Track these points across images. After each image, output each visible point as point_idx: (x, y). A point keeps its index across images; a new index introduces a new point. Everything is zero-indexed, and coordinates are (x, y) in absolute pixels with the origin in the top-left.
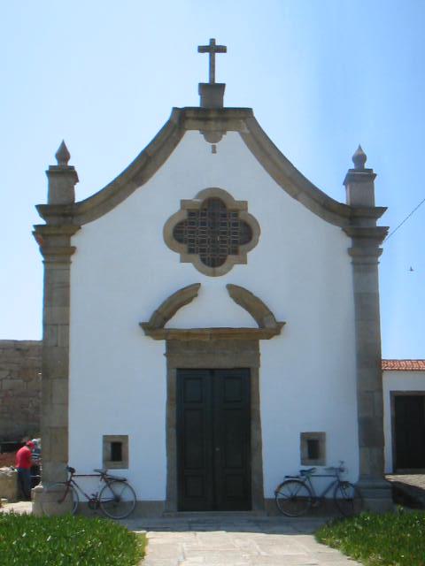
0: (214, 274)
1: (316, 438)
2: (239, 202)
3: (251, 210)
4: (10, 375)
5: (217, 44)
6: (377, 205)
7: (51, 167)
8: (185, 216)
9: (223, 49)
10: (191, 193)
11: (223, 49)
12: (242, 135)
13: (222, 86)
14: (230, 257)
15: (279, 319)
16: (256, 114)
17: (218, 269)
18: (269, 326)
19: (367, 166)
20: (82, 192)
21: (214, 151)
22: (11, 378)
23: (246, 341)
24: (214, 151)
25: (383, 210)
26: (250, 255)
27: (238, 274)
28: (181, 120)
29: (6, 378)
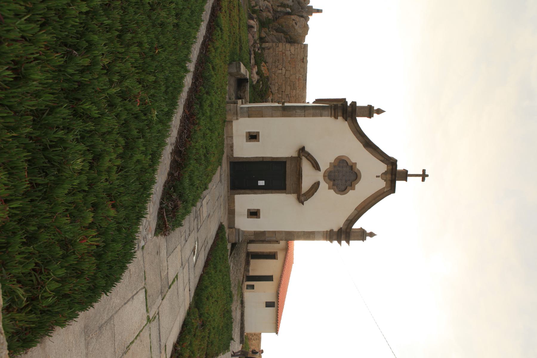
0: (324, 176)
1: (258, 214)
2: (355, 186)
3: (351, 191)
4: (292, 54)
5: (426, 178)
6: (351, 242)
7: (374, 107)
8: (350, 164)
9: (423, 180)
11: (423, 180)
12: (384, 188)
13: (406, 180)
14: (332, 183)
15: (305, 203)
17: (327, 178)
18: (302, 198)
19: (368, 238)
20: (362, 122)
21: (377, 177)
22: (291, 55)
23: (297, 189)
24: (377, 177)
25: (348, 242)
26: (332, 191)
27: (324, 185)
28: (392, 163)
29: (291, 53)
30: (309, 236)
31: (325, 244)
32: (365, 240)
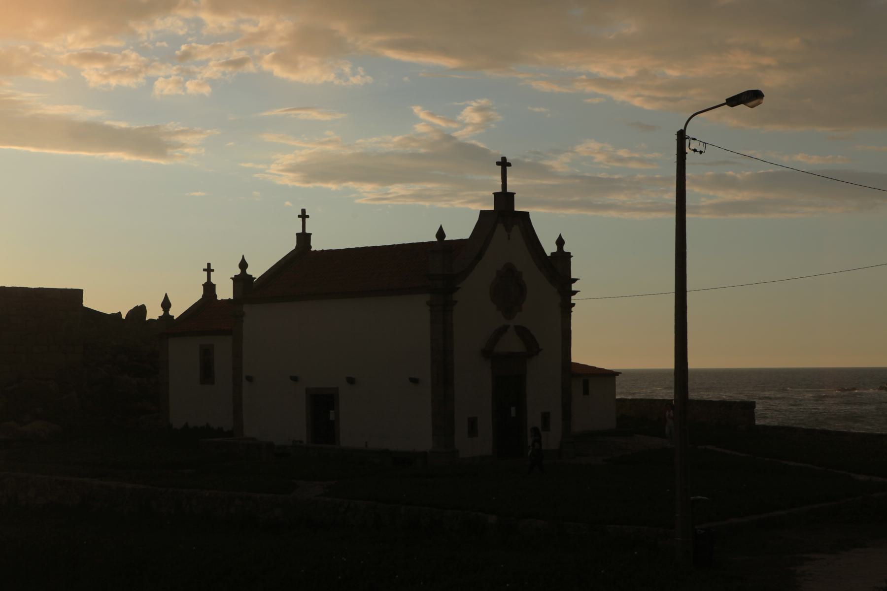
6: (573, 277)
9: (509, 165)
11: (509, 165)
13: (512, 194)
16: (531, 217)
19: (566, 249)
21: (509, 239)
24: (509, 239)
25: (575, 280)
32: (570, 253)
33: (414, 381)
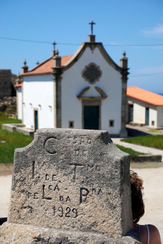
9: (94, 24)
10: (87, 64)
11: (94, 24)
18: (103, 96)
20: (65, 63)
25: (128, 69)
27: (98, 84)
28: (86, 45)
30: (124, 91)
31: (129, 81)
33: (50, 107)
